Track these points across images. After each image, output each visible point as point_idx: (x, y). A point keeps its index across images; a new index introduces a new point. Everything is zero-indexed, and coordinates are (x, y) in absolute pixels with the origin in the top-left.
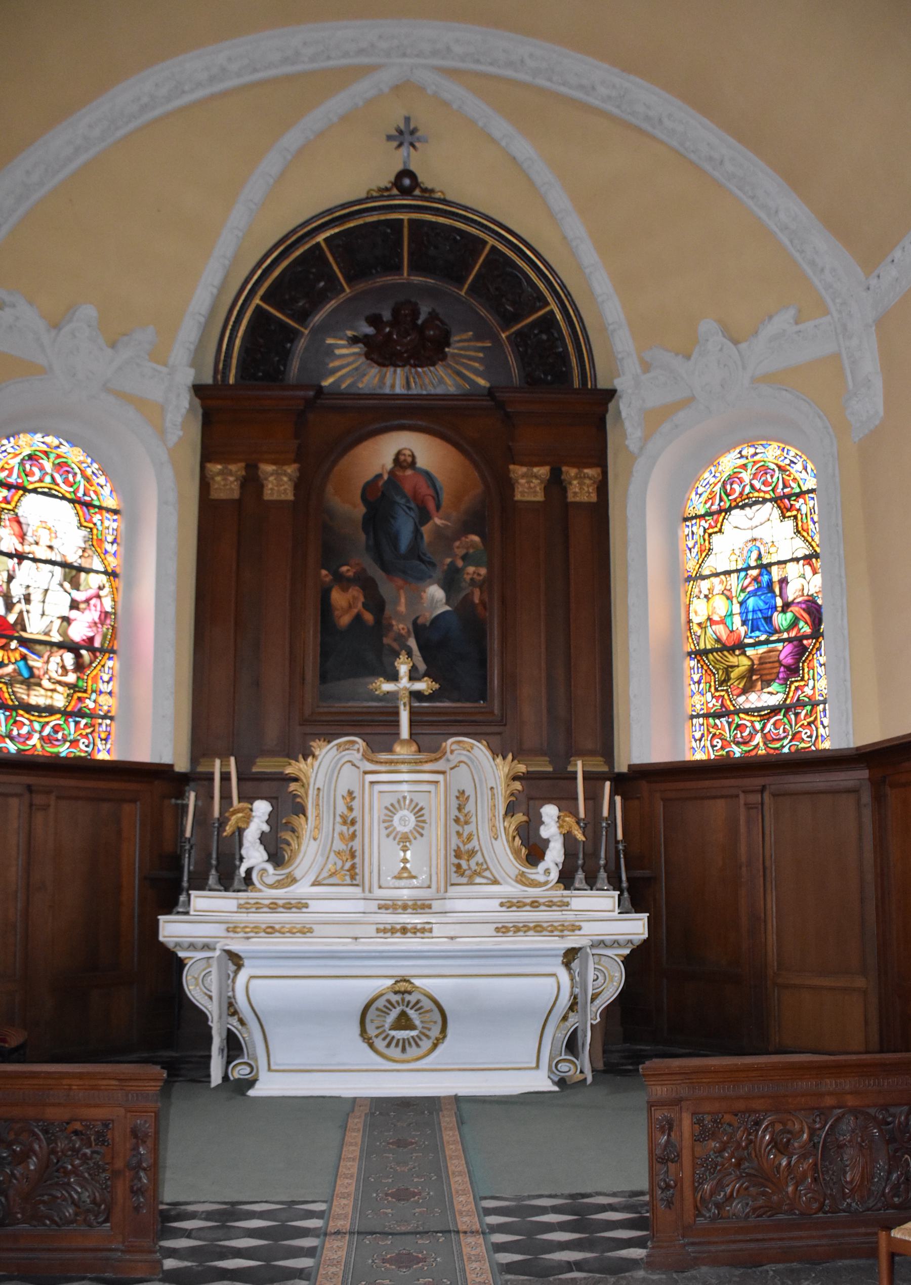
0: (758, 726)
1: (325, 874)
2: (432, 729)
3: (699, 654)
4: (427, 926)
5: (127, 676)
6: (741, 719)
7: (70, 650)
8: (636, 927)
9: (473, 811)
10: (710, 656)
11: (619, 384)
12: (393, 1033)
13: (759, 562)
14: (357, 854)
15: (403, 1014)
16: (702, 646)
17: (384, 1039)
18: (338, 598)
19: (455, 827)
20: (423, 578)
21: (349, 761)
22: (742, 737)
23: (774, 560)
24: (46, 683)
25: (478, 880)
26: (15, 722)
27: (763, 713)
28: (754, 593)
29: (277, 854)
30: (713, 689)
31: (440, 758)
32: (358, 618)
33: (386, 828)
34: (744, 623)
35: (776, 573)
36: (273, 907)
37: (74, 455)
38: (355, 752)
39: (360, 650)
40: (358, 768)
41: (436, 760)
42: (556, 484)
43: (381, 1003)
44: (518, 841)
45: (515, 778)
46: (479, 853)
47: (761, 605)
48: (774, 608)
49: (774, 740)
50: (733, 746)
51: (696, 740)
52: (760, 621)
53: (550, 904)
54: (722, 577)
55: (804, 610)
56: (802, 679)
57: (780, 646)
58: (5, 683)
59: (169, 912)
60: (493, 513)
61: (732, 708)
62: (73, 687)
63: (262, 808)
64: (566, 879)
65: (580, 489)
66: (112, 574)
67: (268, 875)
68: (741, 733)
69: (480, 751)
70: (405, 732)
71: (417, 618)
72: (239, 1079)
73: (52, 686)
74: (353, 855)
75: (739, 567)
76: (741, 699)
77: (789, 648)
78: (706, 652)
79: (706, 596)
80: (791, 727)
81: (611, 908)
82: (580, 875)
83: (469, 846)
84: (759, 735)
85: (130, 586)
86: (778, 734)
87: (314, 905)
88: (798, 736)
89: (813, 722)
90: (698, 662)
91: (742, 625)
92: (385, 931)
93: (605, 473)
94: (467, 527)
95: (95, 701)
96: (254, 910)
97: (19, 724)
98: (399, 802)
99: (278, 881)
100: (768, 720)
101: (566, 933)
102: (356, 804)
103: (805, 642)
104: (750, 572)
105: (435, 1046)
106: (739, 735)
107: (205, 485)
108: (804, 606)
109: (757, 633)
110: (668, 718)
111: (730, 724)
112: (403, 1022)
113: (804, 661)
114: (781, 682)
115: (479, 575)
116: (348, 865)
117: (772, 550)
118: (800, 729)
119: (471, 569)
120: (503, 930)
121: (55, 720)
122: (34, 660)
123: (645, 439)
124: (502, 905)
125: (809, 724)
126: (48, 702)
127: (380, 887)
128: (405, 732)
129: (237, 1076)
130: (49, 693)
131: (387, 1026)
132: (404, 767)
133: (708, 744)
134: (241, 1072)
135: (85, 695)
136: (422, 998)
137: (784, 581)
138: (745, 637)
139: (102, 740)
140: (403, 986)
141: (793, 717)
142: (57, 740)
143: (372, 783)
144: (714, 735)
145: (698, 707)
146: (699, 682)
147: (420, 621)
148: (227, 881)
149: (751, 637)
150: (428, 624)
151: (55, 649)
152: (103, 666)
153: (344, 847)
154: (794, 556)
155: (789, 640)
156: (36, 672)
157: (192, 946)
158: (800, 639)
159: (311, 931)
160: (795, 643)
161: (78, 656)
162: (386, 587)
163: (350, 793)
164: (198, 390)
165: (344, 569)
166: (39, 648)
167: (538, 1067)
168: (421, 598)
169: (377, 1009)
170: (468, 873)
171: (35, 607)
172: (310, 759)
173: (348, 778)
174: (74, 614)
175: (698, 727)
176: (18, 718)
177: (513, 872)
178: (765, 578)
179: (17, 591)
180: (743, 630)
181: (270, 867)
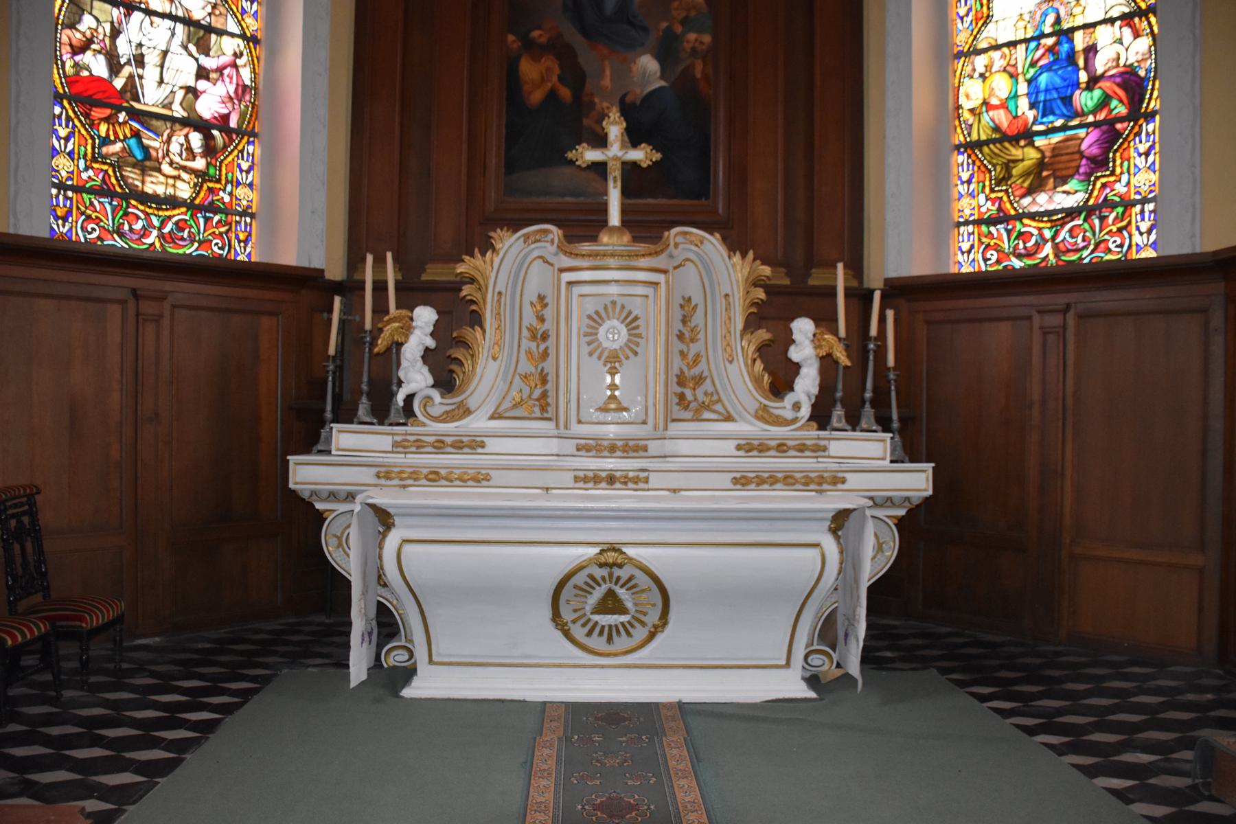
0: (1048, 234)
1: (507, 404)
2: (646, 227)
3: (971, 147)
4: (642, 475)
5: (270, 164)
6: (1025, 225)
7: (197, 129)
8: (917, 481)
9: (701, 325)
10: (986, 149)
12: (596, 618)
13: (1057, 28)
14: (549, 378)
15: (611, 594)
16: (975, 137)
17: (584, 625)
18: (529, 69)
19: (678, 346)
20: (634, 46)
21: (541, 257)
22: (1025, 248)
23: (1079, 22)
24: (166, 168)
25: (707, 415)
26: (126, 214)
27: (1055, 218)
28: (1047, 68)
29: (446, 377)
30: (987, 190)
31: (662, 251)
32: (552, 95)
33: (589, 344)
34: (1032, 106)
35: (1080, 41)
36: (439, 446)
38: (548, 245)
40: (552, 265)
41: (657, 253)
43: (580, 579)
44: (759, 366)
45: (756, 284)
46: (708, 381)
47: (1058, 81)
48: (1077, 85)
49: (1069, 251)
50: (1013, 259)
51: (963, 253)
52: (1056, 102)
53: (801, 448)
54: (1005, 50)
55: (1118, 85)
56: (1113, 173)
57: (1082, 132)
58: (110, 165)
59: (307, 451)
61: (1013, 212)
62: (202, 175)
63: (425, 316)
66: (251, 40)
67: (433, 404)
68: (1024, 243)
69: (713, 245)
70: (614, 218)
71: (625, 95)
72: (395, 667)
73: (175, 173)
74: (544, 381)
75: (1028, 36)
76: (1026, 201)
77: (1095, 135)
78: (979, 144)
79: (982, 75)
80: (1094, 234)
81: (880, 455)
82: (838, 413)
83: (696, 371)
84: (1049, 245)
85: (274, 53)
86: (1076, 243)
87: (493, 445)
88: (1102, 246)
89: (1125, 228)
90: (969, 156)
91: (1030, 109)
92: (585, 480)
95: (231, 194)
96: (413, 449)
97: (131, 217)
98: (606, 308)
99: (447, 412)
100: (1062, 226)
101: (825, 487)
102: (548, 313)
103: (1119, 126)
104: (1043, 41)
105: (652, 636)
106: (1021, 246)
108: (1118, 80)
109: (1051, 118)
110: (942, 220)
111: (1009, 232)
112: (611, 604)
113: (1116, 151)
114: (1082, 178)
115: (702, 43)
116: (537, 393)
117: (1077, 10)
118: (1107, 237)
119: (692, 36)
120: (742, 481)
121: (179, 214)
122: (149, 138)
124: (739, 448)
125: (1120, 230)
126: (170, 191)
127: (580, 422)
128: (614, 218)
129: (391, 662)
130: (171, 181)
131: (588, 608)
132: (611, 262)
133: (980, 257)
134: (397, 658)
135: (218, 186)
136: (638, 573)
137: (1091, 50)
138: (1034, 123)
139: (239, 242)
140: (611, 557)
141: (1097, 222)
142: (182, 239)
143: (570, 283)
144: (988, 246)
145: (967, 212)
146: (969, 182)
147: (629, 99)
148: (381, 413)
149: (1041, 123)
150: (638, 103)
151: (177, 126)
152: (242, 151)
153: (533, 370)
154: (1108, 16)
155: (1096, 125)
156: (153, 153)
157: (333, 496)
158: (1111, 122)
159: (487, 478)
160: (1104, 128)
161: (208, 138)
162: (587, 58)
163: (541, 298)
165: (536, 33)
166: (155, 123)
167: (788, 664)
168: (630, 70)
169: (576, 587)
170: (694, 405)
171: (150, 73)
172: (489, 254)
173: (537, 280)
174: (202, 85)
175: (965, 238)
176: (130, 210)
177: (752, 406)
178: (1066, 47)
179: (124, 48)
180: (1031, 115)
181: (436, 395)
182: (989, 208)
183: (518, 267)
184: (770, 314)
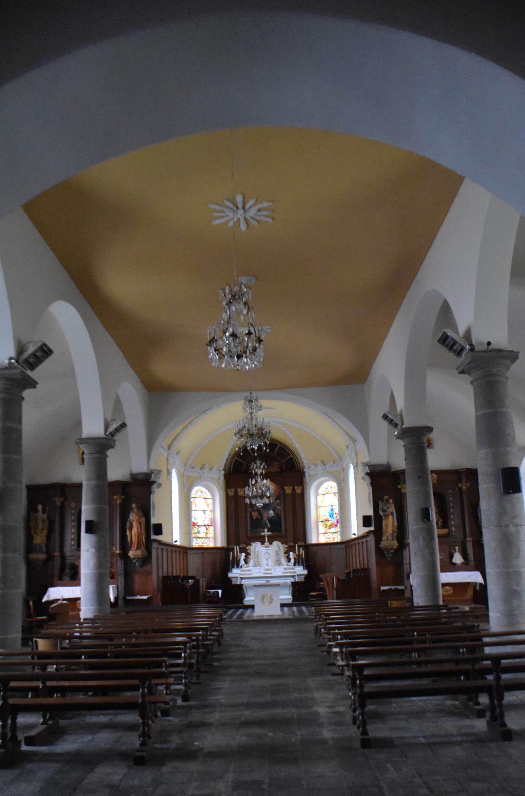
3: (322, 521)
8: (306, 572)
11: (306, 470)
18: (253, 514)
29: (246, 562)
32: (257, 518)
36: (246, 571)
37: (204, 489)
52: (331, 515)
62: (206, 533)
63: (243, 554)
64: (295, 565)
65: (298, 491)
69: (279, 543)
82: (297, 564)
93: (303, 487)
119: (278, 507)
121: (204, 539)
123: (310, 481)
148: (238, 567)
157: (233, 578)
182: (324, 532)
184: (287, 552)
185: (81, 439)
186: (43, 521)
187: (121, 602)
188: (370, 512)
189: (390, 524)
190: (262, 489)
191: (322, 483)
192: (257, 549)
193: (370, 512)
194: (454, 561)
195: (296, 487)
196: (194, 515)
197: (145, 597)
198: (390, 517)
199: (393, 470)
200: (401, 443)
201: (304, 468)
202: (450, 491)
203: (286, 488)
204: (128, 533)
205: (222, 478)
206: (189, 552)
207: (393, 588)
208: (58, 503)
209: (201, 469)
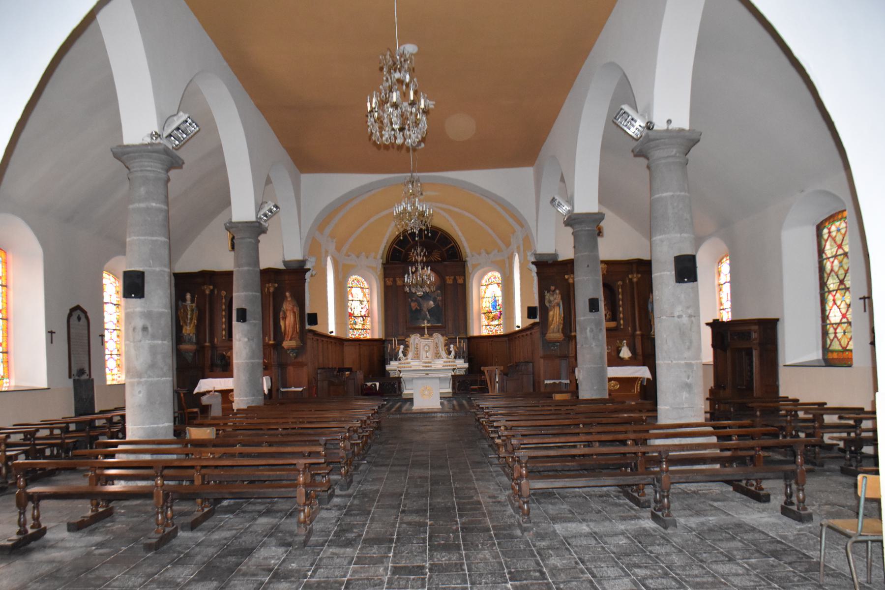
2: (432, 330)
5: (372, 322)
8: (466, 365)
18: (413, 304)
20: (429, 300)
29: (405, 354)
37: (360, 278)
39: (417, 314)
42: (455, 280)
52: (494, 307)
60: (442, 285)
63: (402, 347)
64: (455, 358)
65: (460, 281)
69: (440, 336)
94: (437, 289)
107: (385, 282)
148: (396, 360)
164: (383, 264)
183: (414, 339)
184: (447, 345)
185: (231, 222)
186: (192, 310)
187: (274, 393)
188: (535, 303)
189: (556, 315)
190: (422, 277)
191: (485, 273)
192: (417, 341)
193: (535, 303)
194: (621, 355)
195: (458, 277)
196: (352, 305)
197: (300, 389)
198: (557, 309)
199: (560, 259)
200: (570, 230)
201: (467, 256)
202: (620, 283)
203: (447, 277)
204: (282, 323)
205: (380, 266)
206: (346, 343)
207: (557, 382)
208: (207, 292)
209: (358, 257)
